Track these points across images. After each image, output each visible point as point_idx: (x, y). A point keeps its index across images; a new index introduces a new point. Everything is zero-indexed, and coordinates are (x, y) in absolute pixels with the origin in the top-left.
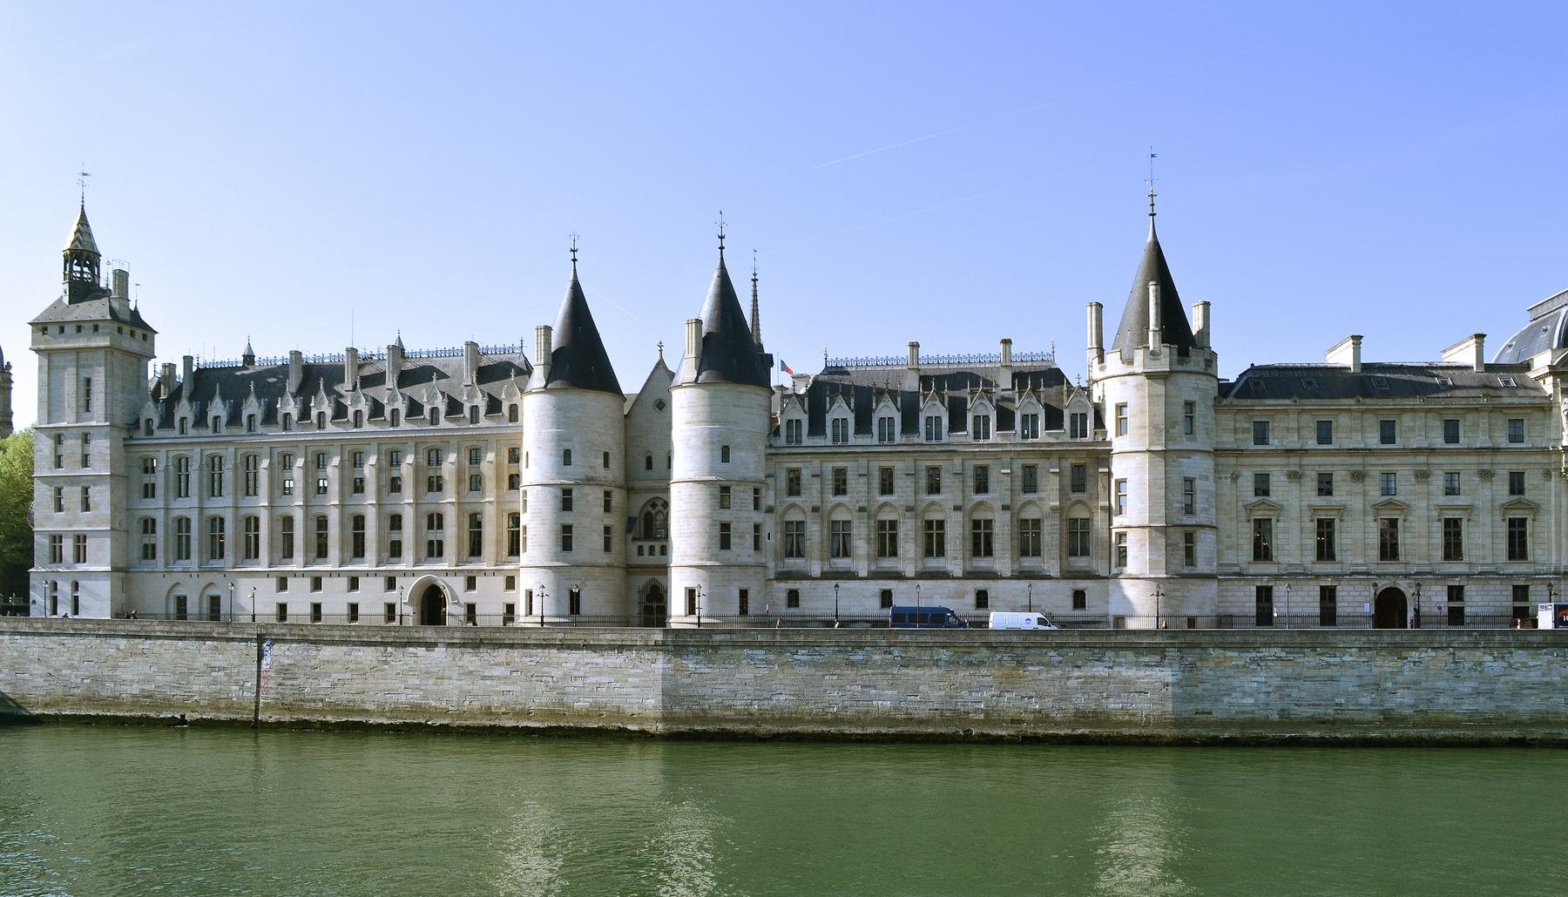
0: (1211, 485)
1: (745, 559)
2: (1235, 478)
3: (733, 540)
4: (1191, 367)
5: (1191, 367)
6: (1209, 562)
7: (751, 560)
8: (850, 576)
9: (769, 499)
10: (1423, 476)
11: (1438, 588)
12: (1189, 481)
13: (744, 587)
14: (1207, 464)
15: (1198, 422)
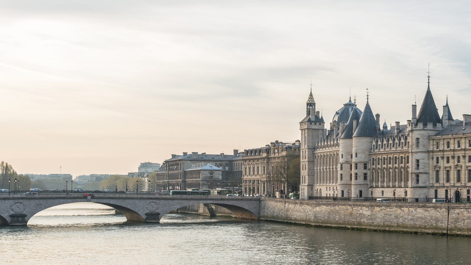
0: (426, 161)
1: (360, 183)
2: (433, 158)
3: (358, 178)
4: (418, 128)
5: (418, 128)
6: (423, 183)
7: (362, 183)
8: (377, 187)
9: (369, 166)
10: (464, 157)
11: (465, 190)
12: (418, 161)
13: (361, 189)
14: (425, 155)
15: (420, 143)
